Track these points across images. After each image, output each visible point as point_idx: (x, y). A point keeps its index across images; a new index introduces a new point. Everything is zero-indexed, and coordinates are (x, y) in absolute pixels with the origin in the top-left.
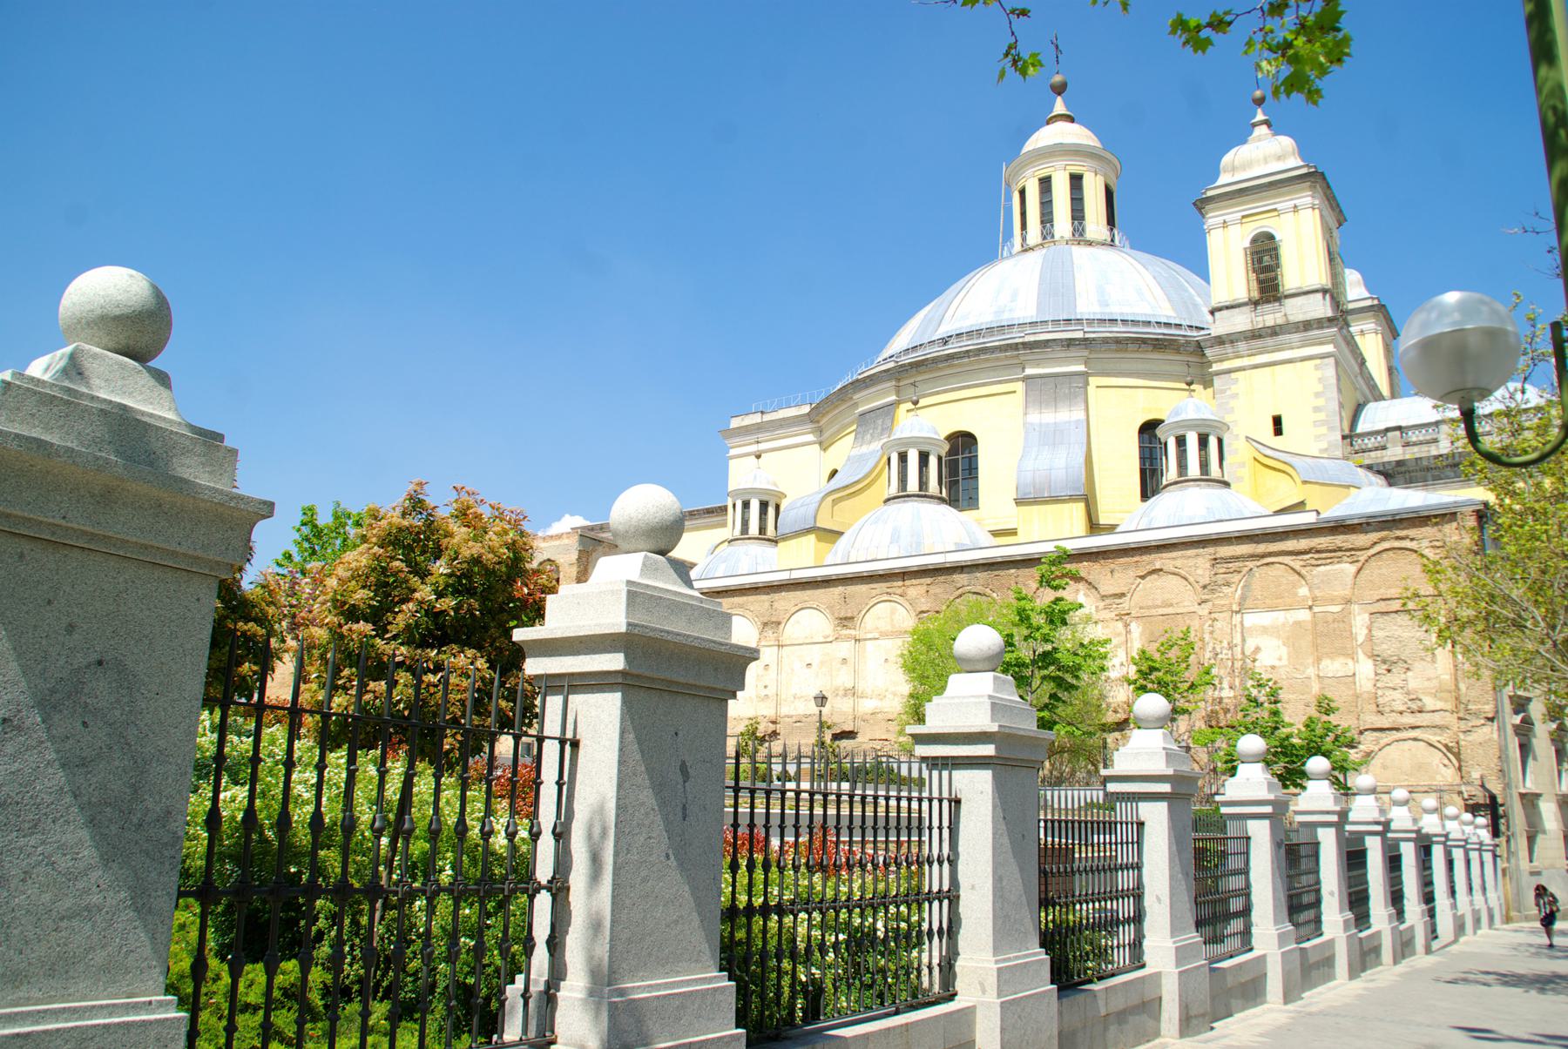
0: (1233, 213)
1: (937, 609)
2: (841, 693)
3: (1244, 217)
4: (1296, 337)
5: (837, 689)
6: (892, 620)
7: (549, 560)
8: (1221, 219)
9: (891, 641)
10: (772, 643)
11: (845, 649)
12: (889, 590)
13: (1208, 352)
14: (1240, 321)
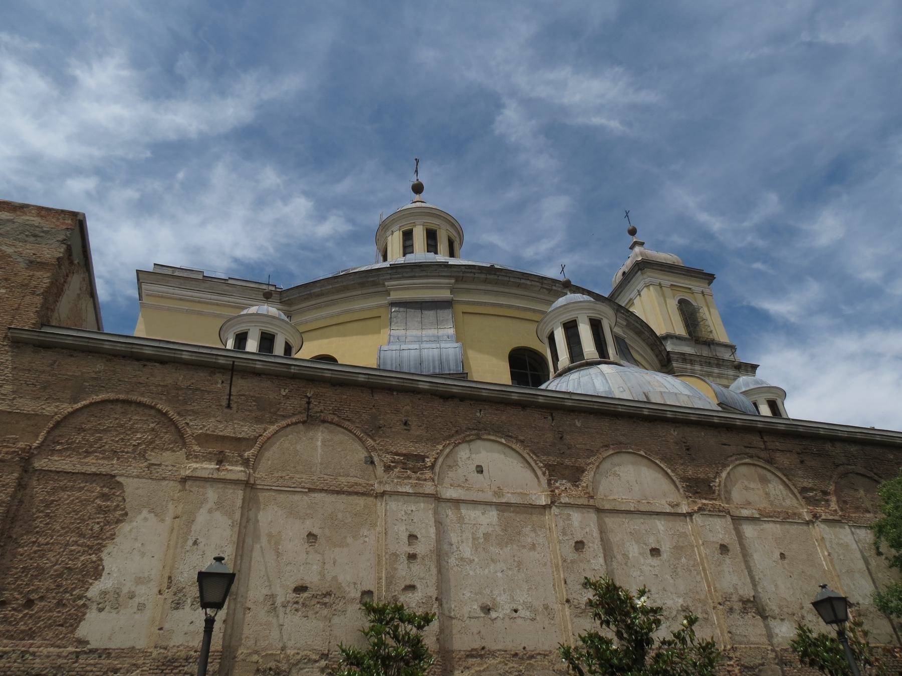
0: (667, 280)
1: (823, 488)
2: (737, 606)
3: (672, 285)
5: (727, 598)
6: (767, 494)
8: (658, 281)
9: (778, 526)
10: (583, 501)
12: (747, 450)
13: (675, 364)
14: (688, 349)
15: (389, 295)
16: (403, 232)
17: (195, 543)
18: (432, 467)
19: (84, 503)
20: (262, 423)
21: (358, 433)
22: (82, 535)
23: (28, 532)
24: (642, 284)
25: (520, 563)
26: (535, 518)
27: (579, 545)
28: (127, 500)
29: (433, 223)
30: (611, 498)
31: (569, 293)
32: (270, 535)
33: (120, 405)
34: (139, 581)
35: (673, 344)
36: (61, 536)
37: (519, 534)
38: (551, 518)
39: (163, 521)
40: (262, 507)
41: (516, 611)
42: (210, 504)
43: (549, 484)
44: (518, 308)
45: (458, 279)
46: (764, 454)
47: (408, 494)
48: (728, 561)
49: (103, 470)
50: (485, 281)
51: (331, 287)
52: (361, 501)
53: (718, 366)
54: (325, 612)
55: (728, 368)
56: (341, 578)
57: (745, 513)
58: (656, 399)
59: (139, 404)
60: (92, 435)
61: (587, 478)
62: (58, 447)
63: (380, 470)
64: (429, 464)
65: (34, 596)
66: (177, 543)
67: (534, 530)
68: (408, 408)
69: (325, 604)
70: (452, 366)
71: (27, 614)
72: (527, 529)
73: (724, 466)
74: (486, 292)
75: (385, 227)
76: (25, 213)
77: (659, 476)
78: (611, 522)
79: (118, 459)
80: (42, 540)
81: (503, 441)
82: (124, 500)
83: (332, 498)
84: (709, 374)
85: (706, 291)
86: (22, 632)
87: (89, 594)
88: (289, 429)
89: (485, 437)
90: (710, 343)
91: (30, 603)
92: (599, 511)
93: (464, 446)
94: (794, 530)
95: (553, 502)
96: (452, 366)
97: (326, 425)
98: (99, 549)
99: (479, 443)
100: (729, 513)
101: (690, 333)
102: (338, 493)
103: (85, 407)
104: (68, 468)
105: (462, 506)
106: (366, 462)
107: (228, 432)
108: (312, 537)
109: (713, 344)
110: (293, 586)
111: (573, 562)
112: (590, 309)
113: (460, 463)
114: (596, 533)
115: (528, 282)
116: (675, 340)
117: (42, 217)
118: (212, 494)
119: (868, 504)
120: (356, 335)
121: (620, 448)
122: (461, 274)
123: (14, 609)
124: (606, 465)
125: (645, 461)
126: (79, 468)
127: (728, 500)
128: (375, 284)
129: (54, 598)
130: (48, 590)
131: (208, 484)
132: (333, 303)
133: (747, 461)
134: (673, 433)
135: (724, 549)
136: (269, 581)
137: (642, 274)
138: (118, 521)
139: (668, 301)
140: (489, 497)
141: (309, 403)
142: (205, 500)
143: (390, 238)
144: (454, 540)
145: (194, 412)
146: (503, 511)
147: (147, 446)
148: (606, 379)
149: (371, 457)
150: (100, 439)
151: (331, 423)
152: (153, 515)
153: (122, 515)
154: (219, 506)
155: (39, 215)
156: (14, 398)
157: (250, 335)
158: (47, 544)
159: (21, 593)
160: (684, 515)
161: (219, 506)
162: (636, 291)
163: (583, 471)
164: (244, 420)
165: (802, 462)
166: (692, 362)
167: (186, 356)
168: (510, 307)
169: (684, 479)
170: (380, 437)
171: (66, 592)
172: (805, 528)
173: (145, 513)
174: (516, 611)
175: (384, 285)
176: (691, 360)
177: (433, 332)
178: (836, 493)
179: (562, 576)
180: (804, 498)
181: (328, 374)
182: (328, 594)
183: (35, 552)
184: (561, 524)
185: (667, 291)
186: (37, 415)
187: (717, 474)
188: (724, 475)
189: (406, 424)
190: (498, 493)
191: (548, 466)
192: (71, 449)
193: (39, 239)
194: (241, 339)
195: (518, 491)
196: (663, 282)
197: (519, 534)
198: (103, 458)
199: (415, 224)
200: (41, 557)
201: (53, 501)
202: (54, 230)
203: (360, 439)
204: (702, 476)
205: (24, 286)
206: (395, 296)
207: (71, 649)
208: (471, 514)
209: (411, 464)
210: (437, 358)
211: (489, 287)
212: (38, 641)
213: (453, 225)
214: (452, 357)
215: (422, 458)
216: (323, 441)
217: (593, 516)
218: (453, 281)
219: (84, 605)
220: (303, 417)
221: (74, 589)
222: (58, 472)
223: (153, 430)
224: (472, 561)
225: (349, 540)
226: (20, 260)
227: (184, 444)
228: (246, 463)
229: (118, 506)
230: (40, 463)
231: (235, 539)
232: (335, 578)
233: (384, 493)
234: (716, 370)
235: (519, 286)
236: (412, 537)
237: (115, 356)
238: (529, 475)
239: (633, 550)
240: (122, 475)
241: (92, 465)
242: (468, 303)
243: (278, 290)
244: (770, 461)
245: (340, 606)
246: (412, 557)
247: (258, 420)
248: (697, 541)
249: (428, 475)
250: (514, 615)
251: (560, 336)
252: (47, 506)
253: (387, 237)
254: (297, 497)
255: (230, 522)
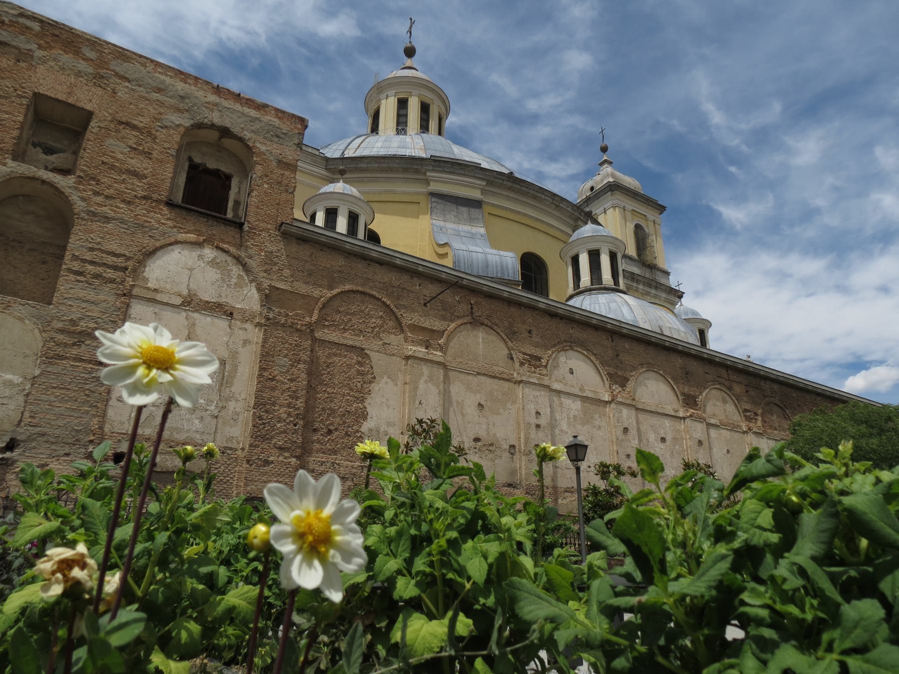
0: (631, 204)
1: (756, 411)
3: (633, 210)
4: (664, 295)
6: (725, 410)
7: (225, 132)
8: (622, 204)
11: (698, 430)
12: (719, 379)
14: (636, 270)
15: (428, 184)
16: (398, 99)
17: (420, 403)
18: (546, 366)
19: (350, 366)
20: (446, 320)
21: (503, 336)
22: (352, 390)
23: (321, 384)
24: (609, 204)
25: (592, 438)
26: (601, 409)
27: (626, 430)
28: (374, 368)
29: (429, 97)
30: (642, 401)
31: (589, 222)
32: (457, 402)
33: (358, 296)
34: (389, 424)
35: (626, 263)
36: (339, 388)
37: (592, 418)
38: (610, 410)
39: (396, 385)
40: (451, 381)
41: (589, 467)
42: (425, 378)
43: (610, 387)
44: (531, 217)
45: (490, 183)
46: (727, 383)
47: (535, 384)
48: (701, 451)
49: (358, 344)
50: (510, 189)
51: (377, 165)
52: (506, 385)
53: (656, 288)
54: (491, 456)
55: (663, 291)
56: (498, 435)
57: (713, 421)
58: (666, 333)
59: (371, 296)
60: (345, 316)
61: (630, 385)
62: (327, 323)
63: (517, 364)
64: (544, 364)
65: (332, 428)
66: (410, 402)
67: (600, 417)
68: (530, 320)
69: (490, 451)
70: (511, 274)
71: (329, 439)
72: (596, 416)
73: (705, 388)
74: (508, 198)
75: (380, 88)
76: (266, 113)
77: (669, 390)
78: (642, 417)
79: (364, 336)
80: (328, 390)
81: (585, 353)
82: (372, 367)
83: (489, 381)
84: (648, 294)
85: (657, 220)
86: (330, 450)
87: (362, 430)
88: (462, 327)
89: (575, 348)
90: (652, 267)
91: (330, 432)
92: (637, 409)
93: (562, 353)
94: (736, 436)
95: (613, 400)
96: (511, 274)
97: (484, 327)
98: (363, 401)
99: (570, 353)
100: (705, 420)
101: (639, 255)
102: (494, 377)
103: (339, 293)
104: (335, 340)
105: (562, 395)
106: (508, 358)
107: (427, 325)
108: (480, 405)
109: (655, 268)
110: (473, 437)
111: (621, 441)
112: (611, 243)
113: (561, 366)
114: (635, 424)
115: (543, 196)
116: (628, 260)
117: (279, 118)
118: (426, 369)
119: (777, 425)
120: (397, 215)
121: (650, 367)
122: (492, 179)
123: (322, 435)
124: (641, 378)
125: (662, 378)
126: (342, 341)
127: (704, 411)
128: (417, 171)
129: (343, 430)
130: (339, 424)
131: (422, 363)
132: (375, 180)
133: (718, 386)
134: (679, 361)
135: (700, 443)
136: (460, 433)
137: (612, 195)
138: (371, 382)
139: (628, 224)
140: (576, 391)
141: (472, 308)
142: (422, 374)
143: (383, 102)
144: (558, 418)
145: (405, 307)
146: (584, 402)
147: (380, 329)
148: (631, 308)
149: (511, 354)
150: (350, 320)
151: (487, 326)
152: (390, 380)
153: (372, 378)
154: (431, 379)
155: (277, 116)
156: (293, 281)
157: (340, 212)
158: (333, 393)
159: (324, 425)
160: (680, 418)
161: (431, 379)
162: (602, 208)
163: (628, 380)
164: (435, 316)
165: (747, 392)
166: (638, 282)
167: (398, 262)
168: (525, 215)
169: (683, 394)
170: (515, 340)
171: (349, 427)
172: (742, 435)
173: (385, 379)
174: (589, 467)
175: (425, 174)
176: (638, 280)
177: (467, 228)
178: (763, 415)
179: (615, 449)
180: (745, 416)
181: (506, 295)
182: (492, 445)
183: (327, 398)
184: (617, 415)
185: (629, 215)
186: (309, 296)
187: (701, 393)
188: (704, 394)
189: (530, 332)
190: (582, 389)
191: (609, 374)
192: (334, 326)
193: (281, 140)
194: (331, 214)
195: (593, 389)
196: (627, 206)
197: (592, 418)
198: (355, 335)
199: (411, 94)
200: (331, 401)
201: (330, 363)
202: (290, 133)
203: (504, 340)
204: (692, 393)
205: (279, 183)
206: (434, 187)
207: (358, 464)
208: (567, 402)
209: (533, 362)
210: (499, 264)
211: (512, 195)
212: (339, 457)
213: (444, 102)
214: (510, 266)
215: (539, 359)
216: (483, 339)
217: (634, 412)
218: (485, 183)
219: (361, 436)
220: (468, 319)
221: (353, 425)
222: (330, 342)
223: (381, 317)
224: (567, 433)
225: (501, 411)
226: (272, 158)
227: (402, 331)
228: (441, 348)
229: (368, 371)
230: (318, 335)
231: (441, 402)
232: (495, 435)
233: (521, 382)
234: (653, 291)
235: (534, 198)
236: (538, 413)
237: (350, 254)
238: (598, 378)
239: (652, 437)
240: (368, 349)
241: (349, 339)
242: (493, 205)
243: (321, 155)
244: (730, 389)
245: (498, 453)
246: (538, 426)
247: (444, 318)
248: (686, 437)
249: (544, 372)
250: (589, 469)
251: (584, 260)
252: (328, 366)
253: (380, 100)
254: (470, 378)
255: (438, 391)
